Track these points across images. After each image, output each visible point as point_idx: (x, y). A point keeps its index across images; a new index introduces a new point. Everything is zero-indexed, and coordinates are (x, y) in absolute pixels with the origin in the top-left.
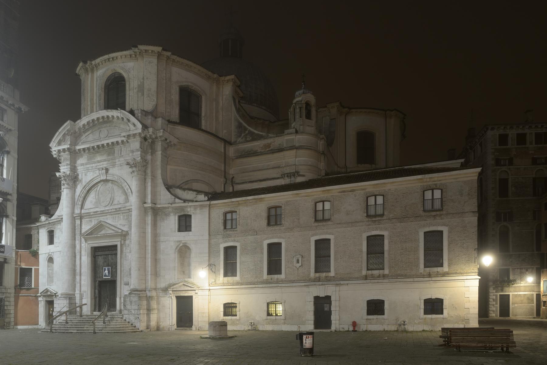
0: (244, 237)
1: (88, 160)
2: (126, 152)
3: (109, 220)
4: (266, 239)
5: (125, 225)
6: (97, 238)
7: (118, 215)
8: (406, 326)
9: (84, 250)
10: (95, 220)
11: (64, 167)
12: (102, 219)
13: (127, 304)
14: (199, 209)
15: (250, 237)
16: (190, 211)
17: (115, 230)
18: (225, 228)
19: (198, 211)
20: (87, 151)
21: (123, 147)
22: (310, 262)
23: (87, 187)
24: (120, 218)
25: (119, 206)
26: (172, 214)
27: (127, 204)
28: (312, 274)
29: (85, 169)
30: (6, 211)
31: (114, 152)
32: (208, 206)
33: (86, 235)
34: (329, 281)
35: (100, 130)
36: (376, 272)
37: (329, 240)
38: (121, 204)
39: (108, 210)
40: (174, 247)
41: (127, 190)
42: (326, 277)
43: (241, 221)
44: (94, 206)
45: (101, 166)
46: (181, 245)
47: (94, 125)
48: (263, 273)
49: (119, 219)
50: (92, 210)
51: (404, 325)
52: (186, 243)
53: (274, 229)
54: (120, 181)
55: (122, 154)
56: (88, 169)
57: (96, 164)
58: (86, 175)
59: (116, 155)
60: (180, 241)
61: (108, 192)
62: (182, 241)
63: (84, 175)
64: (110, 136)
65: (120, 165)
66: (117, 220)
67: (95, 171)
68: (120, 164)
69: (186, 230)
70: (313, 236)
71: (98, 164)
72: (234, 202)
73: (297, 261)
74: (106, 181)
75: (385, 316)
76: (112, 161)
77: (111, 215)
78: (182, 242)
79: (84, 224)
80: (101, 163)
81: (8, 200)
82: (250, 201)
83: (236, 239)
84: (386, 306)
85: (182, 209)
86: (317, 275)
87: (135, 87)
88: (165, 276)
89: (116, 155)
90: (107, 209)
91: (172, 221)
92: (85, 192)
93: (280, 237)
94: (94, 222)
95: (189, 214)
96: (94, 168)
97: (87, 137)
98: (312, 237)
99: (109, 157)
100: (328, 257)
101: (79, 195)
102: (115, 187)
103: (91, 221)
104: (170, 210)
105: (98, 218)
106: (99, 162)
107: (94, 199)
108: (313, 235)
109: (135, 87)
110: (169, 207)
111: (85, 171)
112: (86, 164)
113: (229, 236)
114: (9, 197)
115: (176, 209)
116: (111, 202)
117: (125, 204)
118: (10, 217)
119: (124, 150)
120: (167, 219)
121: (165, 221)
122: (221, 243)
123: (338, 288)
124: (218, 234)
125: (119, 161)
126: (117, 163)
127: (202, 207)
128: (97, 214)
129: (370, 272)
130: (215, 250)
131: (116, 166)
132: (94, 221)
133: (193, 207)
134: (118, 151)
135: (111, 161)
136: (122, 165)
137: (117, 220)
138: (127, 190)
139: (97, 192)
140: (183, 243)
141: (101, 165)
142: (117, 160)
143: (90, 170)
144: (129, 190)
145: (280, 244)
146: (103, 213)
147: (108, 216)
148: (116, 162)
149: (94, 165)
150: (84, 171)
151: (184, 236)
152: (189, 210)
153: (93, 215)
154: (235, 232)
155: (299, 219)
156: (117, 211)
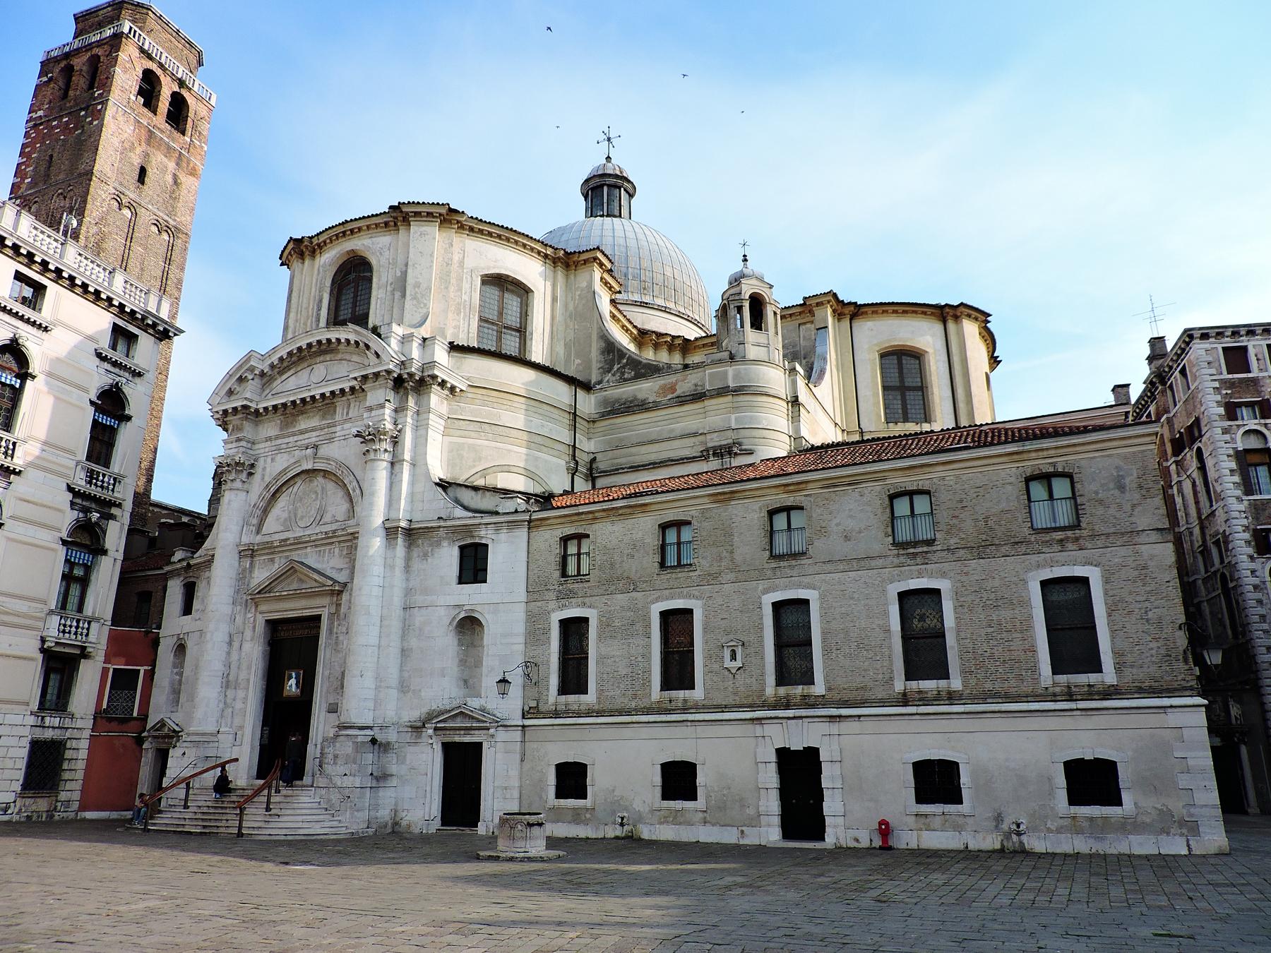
0: (606, 597)
1: (281, 429)
3: (311, 557)
4: (657, 600)
6: (280, 598)
7: (328, 547)
8: (1024, 838)
9: (251, 625)
12: (295, 556)
15: (620, 596)
16: (485, 536)
18: (564, 574)
20: (280, 412)
22: (763, 658)
25: (334, 527)
26: (445, 544)
27: (351, 522)
28: (770, 689)
29: (274, 448)
30: (104, 540)
31: (335, 412)
32: (526, 523)
33: (259, 593)
34: (813, 706)
35: (311, 368)
36: (929, 685)
37: (806, 602)
38: (337, 521)
41: (354, 491)
42: (804, 697)
43: (598, 558)
44: (282, 528)
45: (307, 441)
46: (462, 615)
47: (301, 359)
48: (650, 686)
50: (277, 537)
51: (1019, 834)
53: (674, 576)
56: (279, 449)
57: (296, 438)
59: (338, 417)
61: (314, 496)
63: (269, 460)
69: (476, 581)
70: (767, 593)
71: (301, 437)
72: (582, 513)
73: (732, 656)
75: (965, 807)
77: (316, 546)
80: (307, 435)
81: (113, 517)
82: (620, 512)
83: (587, 600)
84: (965, 779)
85: (467, 530)
86: (782, 691)
90: (307, 533)
91: (448, 558)
92: (268, 496)
93: (689, 596)
94: (278, 565)
98: (764, 594)
100: (805, 645)
101: (255, 505)
102: (330, 486)
103: (272, 560)
104: (442, 532)
105: (288, 554)
106: (302, 432)
108: (766, 591)
109: (389, 282)
110: (440, 527)
112: (277, 437)
113: (570, 595)
114: (114, 511)
116: (319, 518)
118: (109, 553)
121: (429, 560)
122: (553, 610)
123: (835, 728)
124: (547, 590)
126: (337, 435)
127: (513, 525)
129: (914, 685)
133: (493, 526)
138: (354, 491)
139: (292, 496)
142: (338, 428)
144: (358, 491)
145: (689, 612)
146: (299, 543)
147: (309, 548)
149: (291, 439)
151: (472, 595)
152: (483, 533)
153: (277, 547)
154: (586, 585)
155: (732, 552)
156: (329, 539)
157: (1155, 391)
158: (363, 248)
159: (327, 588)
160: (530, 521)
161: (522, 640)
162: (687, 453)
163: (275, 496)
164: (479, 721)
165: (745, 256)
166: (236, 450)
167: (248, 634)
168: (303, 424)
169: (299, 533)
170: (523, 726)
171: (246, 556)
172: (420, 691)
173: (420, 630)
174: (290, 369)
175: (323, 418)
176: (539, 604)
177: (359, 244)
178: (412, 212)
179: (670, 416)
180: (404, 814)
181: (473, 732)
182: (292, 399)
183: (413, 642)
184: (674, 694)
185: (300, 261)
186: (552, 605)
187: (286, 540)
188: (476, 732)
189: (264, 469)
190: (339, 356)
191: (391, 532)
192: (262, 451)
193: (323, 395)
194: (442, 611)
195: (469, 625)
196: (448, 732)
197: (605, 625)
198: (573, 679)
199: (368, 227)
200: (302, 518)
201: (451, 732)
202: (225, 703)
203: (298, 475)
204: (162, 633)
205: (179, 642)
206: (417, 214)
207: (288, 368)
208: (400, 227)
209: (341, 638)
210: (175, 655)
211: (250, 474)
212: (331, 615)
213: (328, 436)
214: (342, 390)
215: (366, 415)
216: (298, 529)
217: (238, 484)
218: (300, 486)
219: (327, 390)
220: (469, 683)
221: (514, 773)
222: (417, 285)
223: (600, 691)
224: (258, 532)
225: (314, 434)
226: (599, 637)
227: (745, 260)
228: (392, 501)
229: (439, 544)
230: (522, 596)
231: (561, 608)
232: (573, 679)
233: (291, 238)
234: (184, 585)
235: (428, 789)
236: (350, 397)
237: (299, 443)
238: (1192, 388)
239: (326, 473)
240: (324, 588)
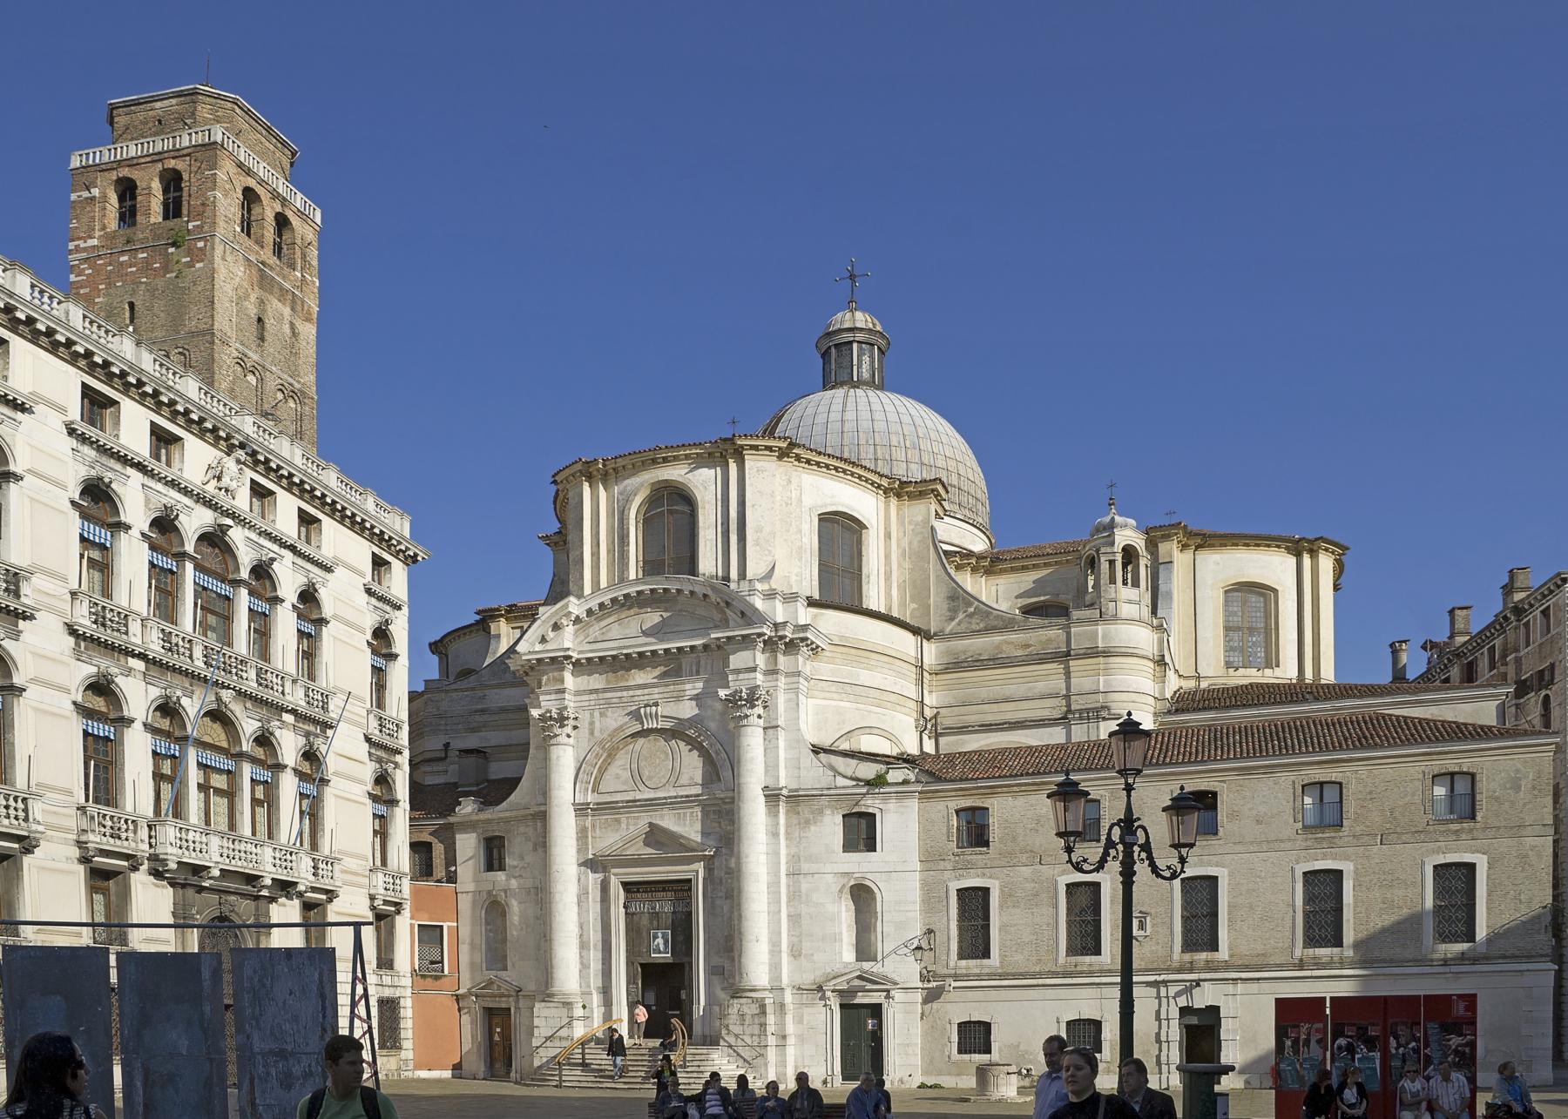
1: (608, 682)
5: (710, 834)
13: (731, 1022)
16: (870, 804)
26: (828, 812)
29: (602, 702)
39: (665, 798)
41: (717, 754)
45: (647, 697)
46: (852, 883)
50: (618, 797)
61: (663, 756)
66: (688, 822)
71: (639, 692)
78: (857, 875)
80: (646, 691)
88: (813, 955)
91: (832, 828)
97: (604, 630)
115: (838, 798)
119: (706, 664)
126: (687, 693)
128: (637, 806)
137: (688, 822)
144: (724, 755)
146: (650, 804)
149: (625, 694)
151: (860, 864)
157: (1507, 625)
163: (611, 755)
166: (558, 702)
168: (640, 677)
173: (807, 895)
177: (675, 473)
182: (625, 651)
183: (804, 909)
184: (1080, 959)
186: (947, 874)
191: (772, 796)
192: (587, 704)
195: (862, 896)
197: (1006, 896)
198: (976, 943)
200: (650, 778)
213: (675, 694)
215: (730, 678)
220: (864, 951)
223: (1003, 957)
225: (656, 690)
226: (1001, 907)
228: (771, 767)
229: (821, 812)
232: (976, 943)
237: (636, 698)
238: (1553, 632)
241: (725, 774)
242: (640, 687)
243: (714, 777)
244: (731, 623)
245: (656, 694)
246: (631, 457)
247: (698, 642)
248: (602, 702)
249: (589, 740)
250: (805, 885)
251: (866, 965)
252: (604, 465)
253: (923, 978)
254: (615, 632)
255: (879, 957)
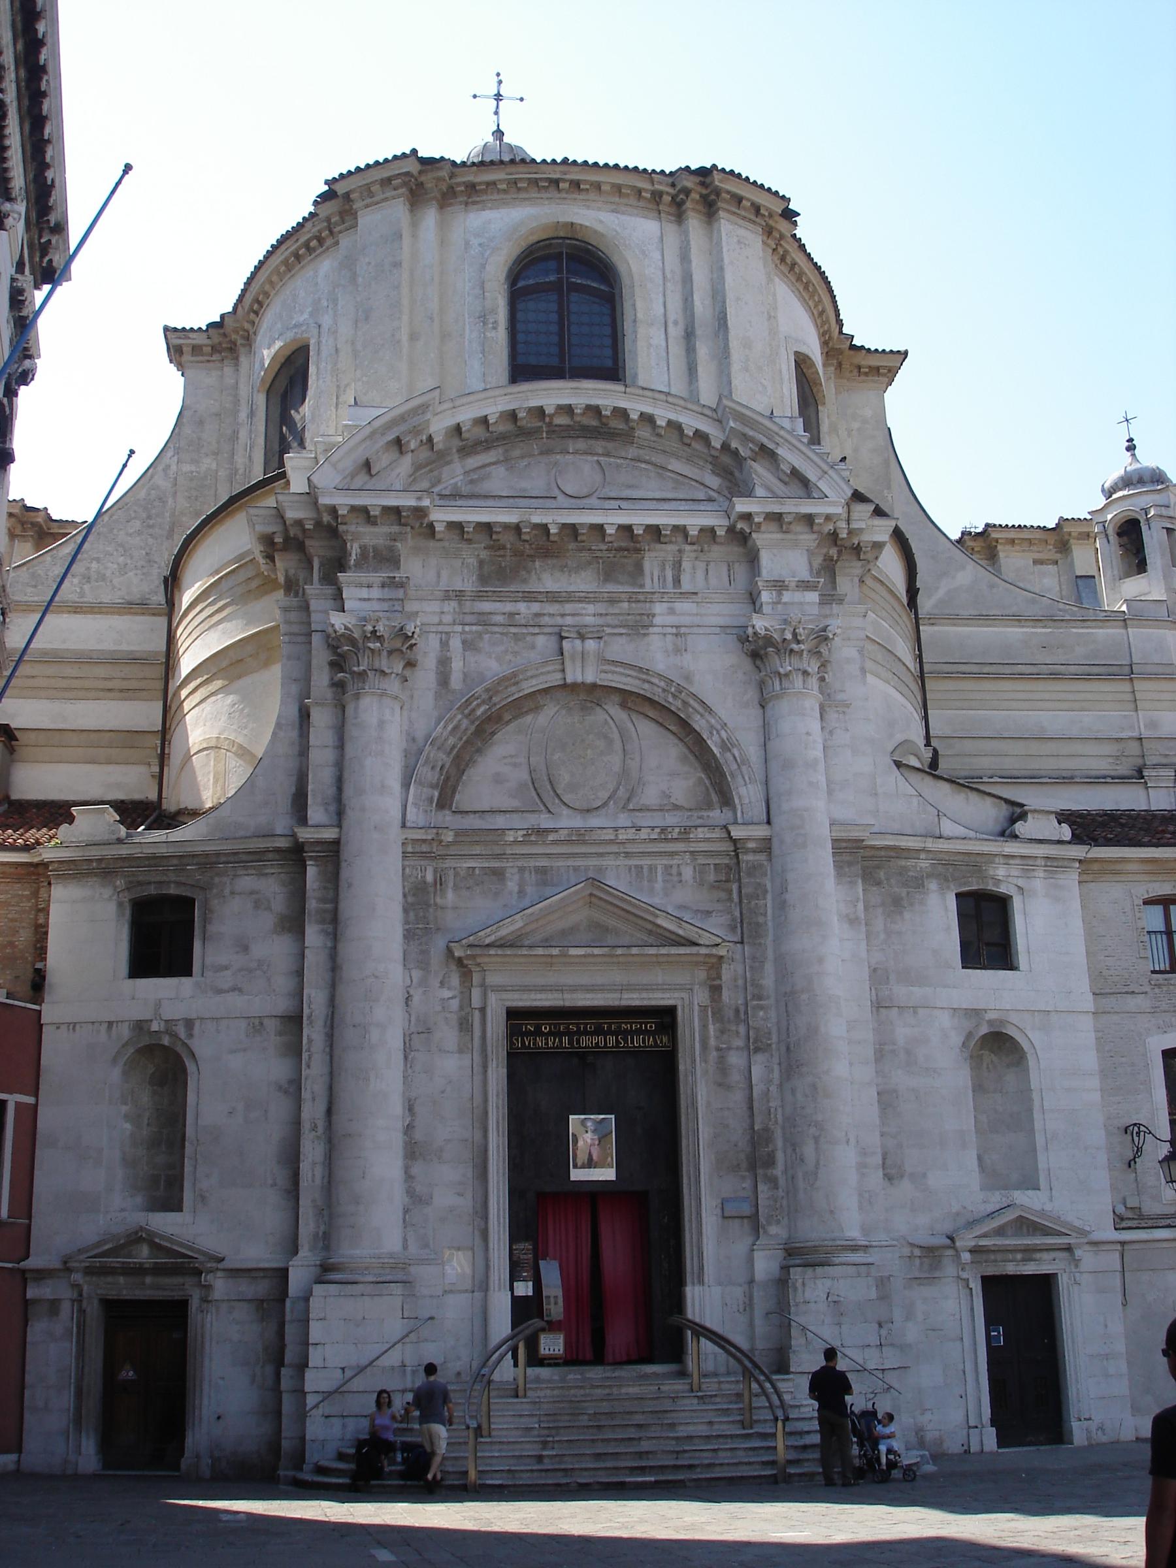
2: (706, 579)
5: (708, 913)
7: (661, 862)
9: (454, 1019)
10: (522, 870)
11: (364, 593)
14: (1042, 875)
17: (681, 932)
19: (1038, 883)
21: (693, 555)
23: (479, 706)
24: (680, 874)
25: (671, 819)
26: (933, 885)
29: (469, 619)
33: (488, 945)
38: (676, 807)
40: (956, 1039)
44: (515, 803)
46: (984, 1030)
49: (676, 879)
50: (500, 822)
52: (1001, 1021)
54: (679, 704)
55: (686, 586)
57: (536, 607)
58: (468, 645)
60: (975, 1013)
62: (985, 1011)
63: (456, 643)
64: (613, 495)
65: (674, 630)
66: (659, 885)
67: (528, 638)
68: (677, 627)
74: (593, 694)
76: (633, 605)
77: (628, 855)
79: (451, 884)
80: (569, 608)
85: (976, 863)
87: (672, 317)
89: (648, 581)
90: (594, 821)
95: (1003, 889)
96: (523, 622)
99: (611, 587)
107: (515, 765)
110: (923, 850)
111: (467, 628)
112: (479, 596)
116: (621, 792)
117: (705, 814)
119: (694, 568)
120: (912, 904)
121: (907, 915)
125: (672, 612)
126: (658, 620)
130: (1124, 1059)
131: (651, 630)
132: (517, 877)
133: (1018, 861)
134: (663, 569)
135: (626, 605)
136: (683, 630)
137: (659, 885)
140: (991, 1023)
141: (563, 615)
142: (658, 608)
143: (496, 629)
148: (654, 615)
149: (522, 607)
150: (459, 628)
158: (599, 228)
159: (703, 951)
160: (1080, 861)
161: (1095, 1082)
162: (1102, 766)
164: (1046, 1231)
165: (1131, 440)
167: (448, 1035)
168: (549, 581)
169: (568, 821)
170: (1123, 1243)
171: (424, 855)
172: (924, 1175)
174: (488, 449)
175: (609, 575)
176: (1115, 1018)
178: (728, 192)
179: (1071, 697)
180: (928, 1416)
181: (1038, 1255)
182: (536, 519)
185: (408, 206)
187: (542, 832)
188: (1045, 1256)
189: (444, 663)
190: (632, 452)
193: (627, 529)
194: (945, 1020)
196: (992, 1257)
199: (618, 189)
201: (999, 1257)
202: (410, 1192)
203: (546, 691)
204: (50, 1012)
205: (146, 1041)
206: (739, 200)
207: (484, 445)
208: (690, 214)
209: (736, 1059)
210: (125, 1073)
211: (411, 664)
212: (703, 1009)
214: (681, 530)
215: (765, 597)
216: (565, 811)
217: (393, 686)
218: (549, 716)
219: (640, 519)
221: (1117, 1327)
222: (747, 344)
224: (444, 802)
225: (591, 608)
227: (1131, 448)
229: (918, 883)
230: (1088, 1002)
231: (1164, 1029)
233: (414, 152)
234: (130, 900)
235: (969, 1367)
236: (688, 548)
239: (629, 700)
240: (694, 950)
241: (743, 791)
242: (553, 597)
243: (714, 797)
244: (760, 491)
245: (589, 615)
246: (512, 169)
247: (694, 521)
248: (469, 619)
249: (438, 696)
250: (902, 1032)
251: (1023, 1198)
252: (452, 175)
253: (1120, 1223)
254: (499, 481)
255: (1043, 1182)
